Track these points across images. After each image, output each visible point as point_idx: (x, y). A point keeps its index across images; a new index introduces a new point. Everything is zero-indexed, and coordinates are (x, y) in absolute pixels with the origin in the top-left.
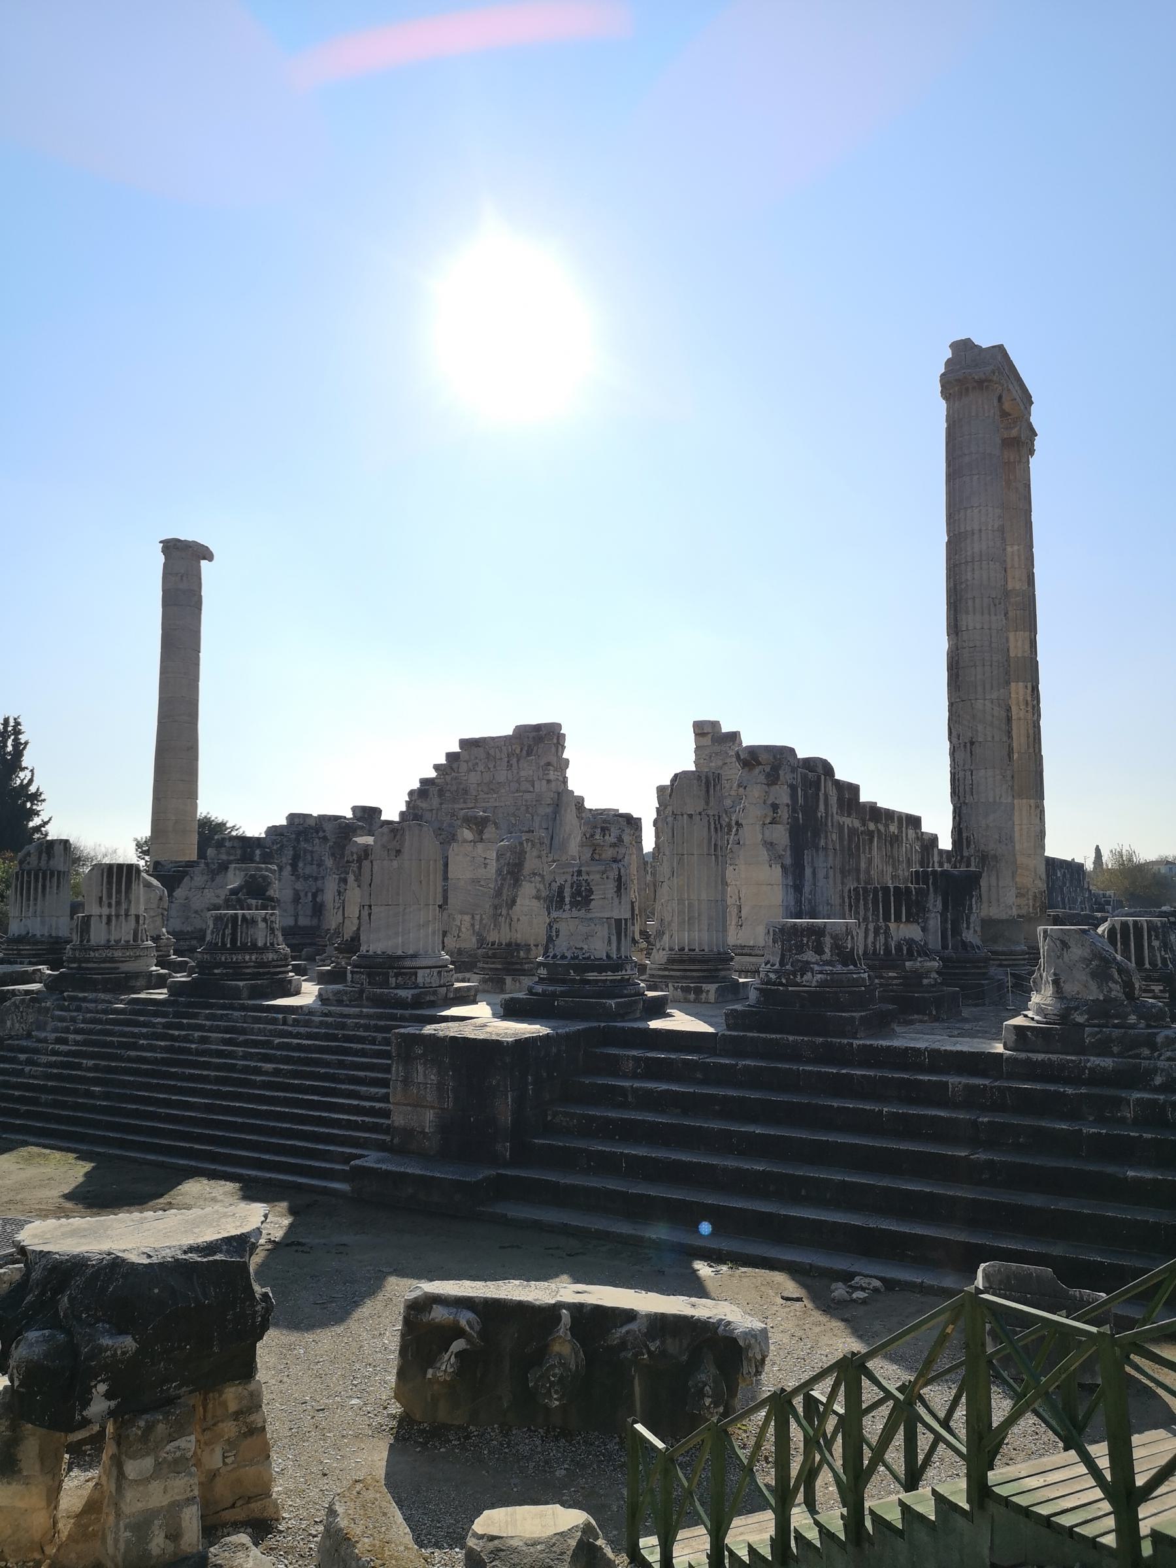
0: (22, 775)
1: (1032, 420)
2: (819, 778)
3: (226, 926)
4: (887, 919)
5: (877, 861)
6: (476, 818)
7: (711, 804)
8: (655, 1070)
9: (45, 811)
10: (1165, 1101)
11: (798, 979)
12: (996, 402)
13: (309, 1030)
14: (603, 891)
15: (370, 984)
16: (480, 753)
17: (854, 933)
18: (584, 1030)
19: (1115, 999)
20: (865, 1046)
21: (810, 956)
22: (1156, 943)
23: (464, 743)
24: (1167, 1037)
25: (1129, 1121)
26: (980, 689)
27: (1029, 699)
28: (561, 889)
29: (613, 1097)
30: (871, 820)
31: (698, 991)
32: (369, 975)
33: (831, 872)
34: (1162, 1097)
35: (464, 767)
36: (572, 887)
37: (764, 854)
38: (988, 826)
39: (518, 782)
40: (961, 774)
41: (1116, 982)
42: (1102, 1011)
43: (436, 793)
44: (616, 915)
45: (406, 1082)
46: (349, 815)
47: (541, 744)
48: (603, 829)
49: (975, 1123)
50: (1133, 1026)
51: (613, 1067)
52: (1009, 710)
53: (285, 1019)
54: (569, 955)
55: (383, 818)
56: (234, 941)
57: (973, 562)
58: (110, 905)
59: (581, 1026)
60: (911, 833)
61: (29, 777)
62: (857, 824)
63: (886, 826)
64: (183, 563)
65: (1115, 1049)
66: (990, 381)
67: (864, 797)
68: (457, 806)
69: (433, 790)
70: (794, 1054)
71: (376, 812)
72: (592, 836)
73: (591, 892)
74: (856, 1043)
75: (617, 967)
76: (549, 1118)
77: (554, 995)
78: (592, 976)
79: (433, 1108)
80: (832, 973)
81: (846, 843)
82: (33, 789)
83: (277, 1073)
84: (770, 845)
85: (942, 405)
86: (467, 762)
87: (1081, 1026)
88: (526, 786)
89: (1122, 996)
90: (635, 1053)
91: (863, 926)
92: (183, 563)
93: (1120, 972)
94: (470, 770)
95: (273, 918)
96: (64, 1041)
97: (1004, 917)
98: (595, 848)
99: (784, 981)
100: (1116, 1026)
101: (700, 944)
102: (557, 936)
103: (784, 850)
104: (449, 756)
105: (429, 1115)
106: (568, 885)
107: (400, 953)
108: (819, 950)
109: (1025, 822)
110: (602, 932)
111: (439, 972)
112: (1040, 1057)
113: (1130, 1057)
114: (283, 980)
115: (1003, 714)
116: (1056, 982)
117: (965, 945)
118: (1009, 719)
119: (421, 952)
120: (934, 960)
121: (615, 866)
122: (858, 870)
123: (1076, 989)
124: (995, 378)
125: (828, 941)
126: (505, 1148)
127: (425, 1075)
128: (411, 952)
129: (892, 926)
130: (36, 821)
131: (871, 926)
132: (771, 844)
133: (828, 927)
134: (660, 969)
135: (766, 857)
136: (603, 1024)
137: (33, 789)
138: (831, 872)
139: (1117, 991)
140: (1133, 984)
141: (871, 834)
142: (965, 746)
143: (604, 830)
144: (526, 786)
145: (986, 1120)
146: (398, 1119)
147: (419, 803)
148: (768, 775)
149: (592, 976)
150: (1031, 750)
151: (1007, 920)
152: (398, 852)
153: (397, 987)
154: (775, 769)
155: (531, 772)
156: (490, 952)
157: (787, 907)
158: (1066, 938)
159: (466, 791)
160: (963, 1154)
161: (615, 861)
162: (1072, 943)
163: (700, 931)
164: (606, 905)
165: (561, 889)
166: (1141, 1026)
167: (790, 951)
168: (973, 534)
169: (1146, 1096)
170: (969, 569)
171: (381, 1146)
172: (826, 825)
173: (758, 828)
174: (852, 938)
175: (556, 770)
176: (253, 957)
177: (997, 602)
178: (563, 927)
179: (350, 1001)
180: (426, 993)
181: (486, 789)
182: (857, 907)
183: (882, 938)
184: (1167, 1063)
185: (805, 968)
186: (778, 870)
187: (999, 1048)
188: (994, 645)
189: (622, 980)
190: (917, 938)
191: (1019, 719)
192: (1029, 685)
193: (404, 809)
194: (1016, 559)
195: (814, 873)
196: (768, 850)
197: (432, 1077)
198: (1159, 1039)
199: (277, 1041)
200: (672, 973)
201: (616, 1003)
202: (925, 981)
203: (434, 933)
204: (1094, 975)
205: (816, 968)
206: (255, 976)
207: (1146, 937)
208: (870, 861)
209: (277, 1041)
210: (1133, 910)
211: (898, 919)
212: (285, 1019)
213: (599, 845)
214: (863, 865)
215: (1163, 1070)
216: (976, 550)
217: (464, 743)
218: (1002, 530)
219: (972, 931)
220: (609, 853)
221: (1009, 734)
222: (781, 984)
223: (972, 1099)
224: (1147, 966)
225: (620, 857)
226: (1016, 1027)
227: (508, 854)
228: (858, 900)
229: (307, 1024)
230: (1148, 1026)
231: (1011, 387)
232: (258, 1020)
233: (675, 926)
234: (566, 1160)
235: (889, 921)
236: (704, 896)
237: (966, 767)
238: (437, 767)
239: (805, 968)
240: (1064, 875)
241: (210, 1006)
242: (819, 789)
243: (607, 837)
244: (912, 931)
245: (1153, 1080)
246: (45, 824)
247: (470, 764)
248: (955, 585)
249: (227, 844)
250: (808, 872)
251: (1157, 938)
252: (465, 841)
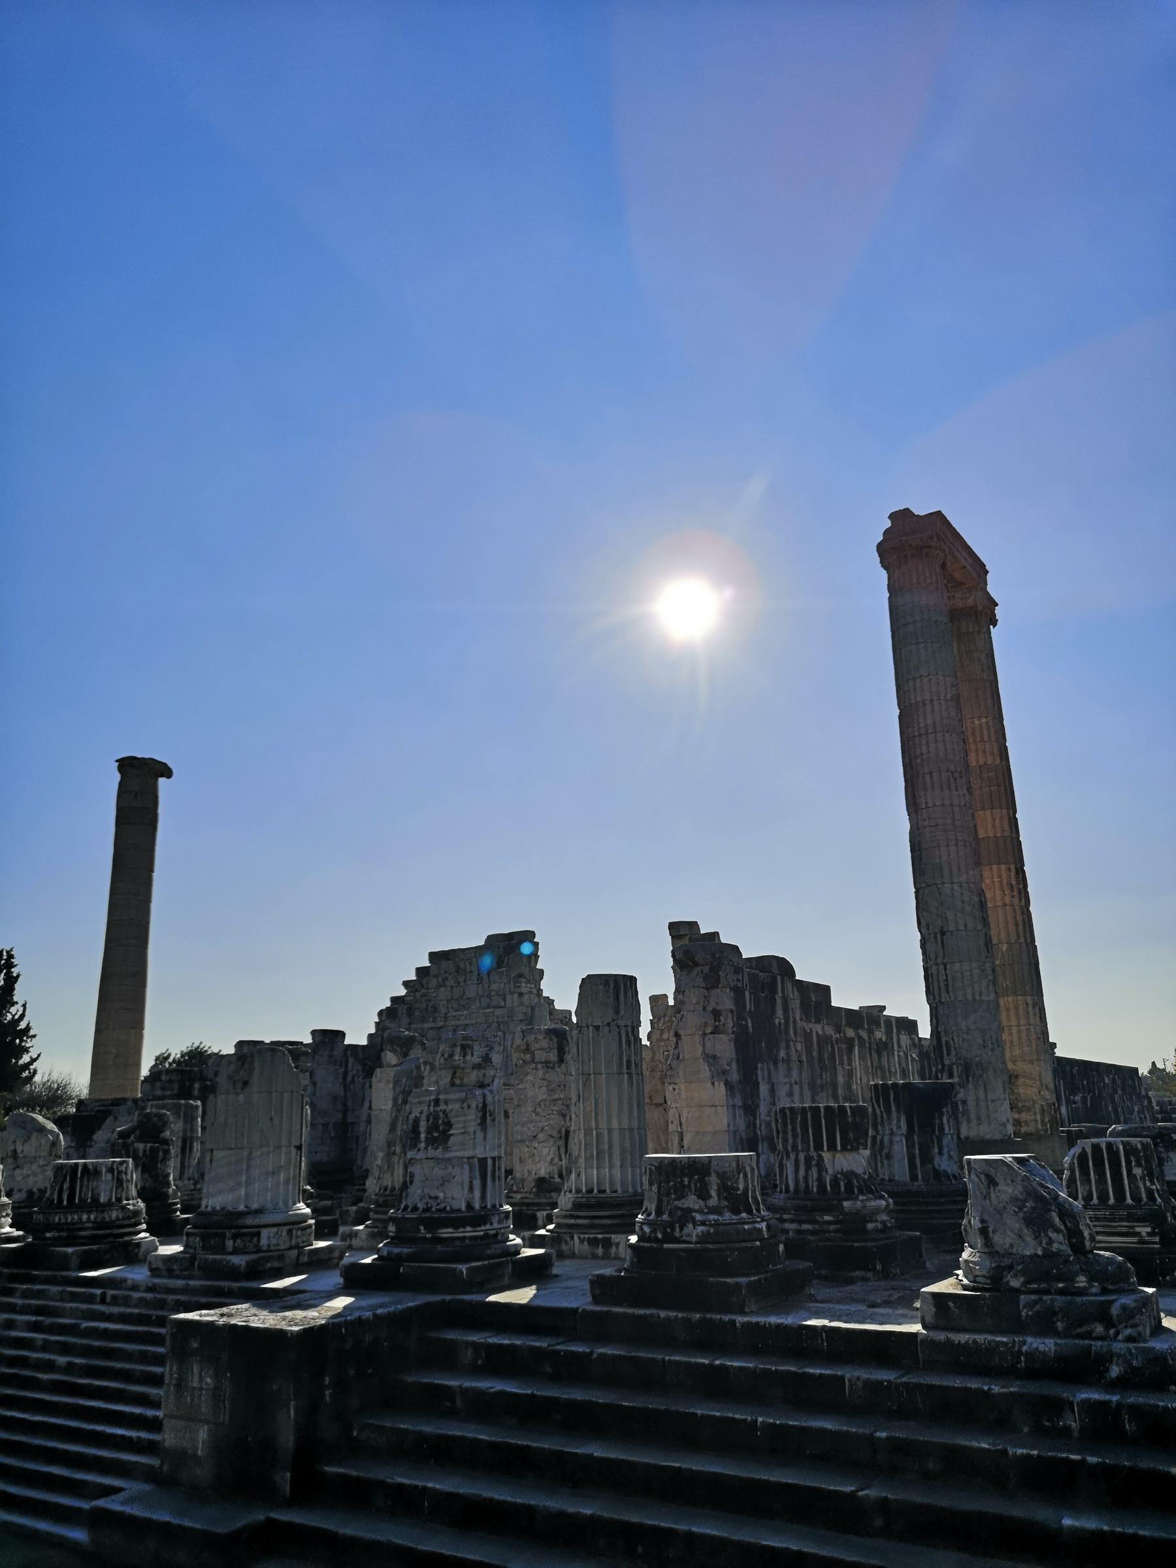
0: (13, 1010)
1: (989, 589)
2: (774, 979)
3: (65, 1179)
4: (819, 1147)
5: (859, 1073)
6: (400, 1038)
7: (622, 1012)
8: (497, 1362)
9: (35, 1047)
10: (1119, 1404)
11: (677, 1234)
12: (938, 570)
13: (122, 1310)
14: (465, 1122)
15: (203, 1248)
17: (748, 1169)
18: (418, 1308)
19: (1058, 1254)
20: (749, 1324)
21: (691, 1201)
22: (1138, 1171)
23: (433, 956)
24: (1124, 1308)
25: (1076, 1434)
26: (946, 872)
27: (1014, 882)
28: (417, 1121)
29: (438, 1402)
30: (849, 1025)
31: (607, 1244)
32: (204, 1238)
33: (796, 1088)
34: (1115, 1398)
35: (433, 982)
36: (428, 1120)
37: (705, 1070)
38: (969, 1029)
39: (489, 996)
40: (934, 968)
41: (1058, 1231)
42: (1043, 1271)
43: (405, 1012)
44: (479, 1153)
45: (180, 1385)
46: (308, 1039)
47: (511, 953)
48: (464, 1048)
49: (871, 1440)
50: (1082, 1292)
51: (447, 1358)
52: (981, 894)
53: (103, 1295)
54: (421, 1206)
55: (346, 1042)
57: (927, 733)
59: (412, 1301)
60: (905, 1039)
61: (20, 1012)
62: (829, 1030)
63: (870, 1032)
64: (140, 781)
65: (1060, 1325)
66: (930, 547)
67: (835, 1002)
68: (426, 1025)
69: (402, 1009)
70: (663, 1336)
71: (341, 1035)
72: (451, 1056)
73: (449, 1125)
74: (740, 1319)
75: (478, 1218)
76: (355, 1434)
77: (398, 1259)
78: (446, 1233)
79: (206, 1422)
80: (717, 1224)
81: (815, 1054)
82: (23, 1025)
83: (70, 1368)
84: (711, 1059)
85: (884, 575)
87: (1017, 1291)
88: (497, 1000)
89: (1066, 1248)
90: (476, 1338)
91: (793, 1156)
92: (140, 781)
93: (1062, 1216)
94: (439, 986)
95: (123, 1168)
97: (998, 1137)
98: (455, 1070)
99: (660, 1236)
100: (1061, 1292)
101: (612, 1183)
102: (411, 1182)
103: (729, 1064)
104: (420, 971)
105: (203, 1433)
106: (424, 1117)
107: (242, 1208)
108: (703, 1195)
109: (1023, 1022)
110: (462, 1175)
111: (290, 1232)
112: (963, 1338)
113: (1079, 1336)
114: (129, 1243)
115: (977, 899)
116: (984, 1231)
117: (937, 1174)
118: (983, 905)
119: (269, 1205)
120: (882, 1197)
121: (478, 1092)
122: (835, 1086)
123: (1008, 1241)
124: (933, 544)
125: (713, 1181)
126: (284, 1479)
127: (201, 1379)
128: (255, 1206)
129: (826, 1156)
130: (26, 1058)
131: (802, 1156)
132: (714, 1057)
133: (714, 1163)
134: (565, 1217)
135: (708, 1074)
136: (448, 1298)
137: (23, 1025)
138: (796, 1088)
139: (1059, 1243)
140: (1081, 1233)
141: (850, 1043)
142: (936, 937)
143: (464, 1048)
144: (497, 1000)
145: (884, 1435)
146: (168, 1438)
147: (387, 1023)
148: (706, 978)
149: (446, 1233)
150: (1022, 940)
151: (1002, 1141)
152: (245, 1084)
153: (235, 1252)
154: (715, 969)
156: (381, 1200)
157: (735, 1133)
158: (992, 1172)
159: (435, 1009)
160: (849, 1489)
161: (482, 1085)
162: (999, 1179)
163: (611, 1167)
164: (469, 1142)
165: (417, 1121)
166: (1094, 1290)
167: (668, 1194)
168: (924, 705)
169: (1096, 1396)
170: (924, 741)
171: (150, 1475)
172: (787, 1033)
173: (697, 1038)
174: (746, 1176)
175: (529, 982)
176: (92, 1217)
177: (957, 775)
178: (415, 1169)
179: (182, 1270)
180: (267, 1259)
182: (785, 1133)
183: (814, 1171)
184: (1123, 1345)
185: (685, 1217)
186: (721, 1089)
187: (916, 1328)
188: (958, 823)
189: (486, 1236)
190: (860, 1171)
191: (1005, 905)
192: (1012, 867)
193: (373, 1031)
194: (985, 732)
195: (772, 1091)
196: (710, 1065)
197: (209, 1380)
198: (1115, 1310)
199: (85, 1324)
200: (579, 1221)
201: (468, 1269)
202: (870, 1226)
203: (287, 1182)
204: (1029, 1222)
205: (698, 1217)
206: (94, 1239)
207: (1124, 1164)
208: (850, 1074)
209: (85, 1324)
210: (126, 1238)
211: (832, 1147)
212: (103, 1295)
213: (458, 1067)
214: (841, 1079)
215: (1119, 1356)
216: (929, 721)
217: (433, 956)
218: (957, 699)
219: (946, 1156)
220: (473, 1076)
221: (985, 922)
222: (657, 1240)
223: (874, 1402)
224: (1129, 1201)
225: (487, 1081)
226: (935, 1296)
227: (404, 1080)
228: (785, 1124)
229: (126, 1301)
230: (1105, 1291)
231: (957, 554)
232: (75, 1297)
233: (582, 1160)
234: (358, 1496)
235: (822, 1149)
236: (615, 1124)
237: (939, 961)
238: (406, 984)
239: (685, 1217)
240: (1114, 1081)
241: (32, 1280)
242: (774, 991)
243: (468, 1057)
244: (857, 1161)
245: (1107, 1370)
246: (33, 1060)
247: (440, 979)
248: (910, 760)
249: (164, 1078)
250: (764, 1089)
251: (1139, 1165)
252: (389, 1066)
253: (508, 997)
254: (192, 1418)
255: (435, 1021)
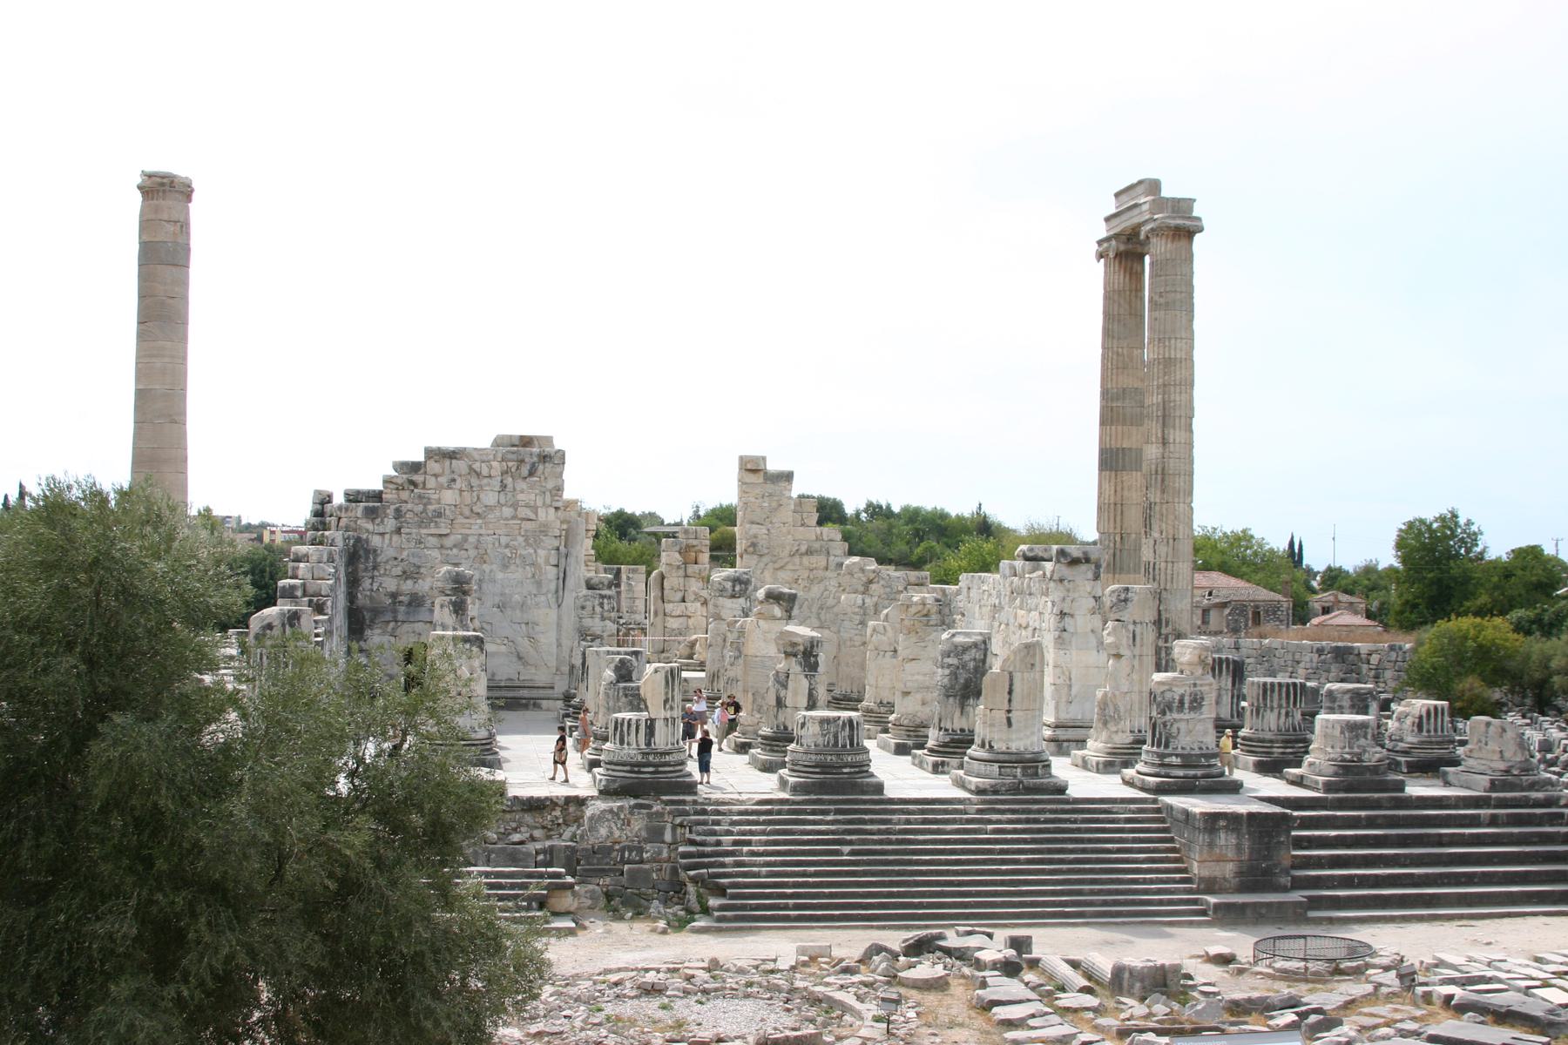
16: (460, 465)
23: (431, 453)
35: (431, 482)
45: (1211, 845)
56: (852, 744)
58: (672, 708)
68: (424, 531)
77: (1195, 777)
86: (436, 476)
94: (440, 487)
96: (749, 843)
155: (533, 497)
178: (1183, 726)
181: (467, 512)
228: (1272, 691)
253: (541, 513)
254: (1220, 860)
255: (437, 526)
